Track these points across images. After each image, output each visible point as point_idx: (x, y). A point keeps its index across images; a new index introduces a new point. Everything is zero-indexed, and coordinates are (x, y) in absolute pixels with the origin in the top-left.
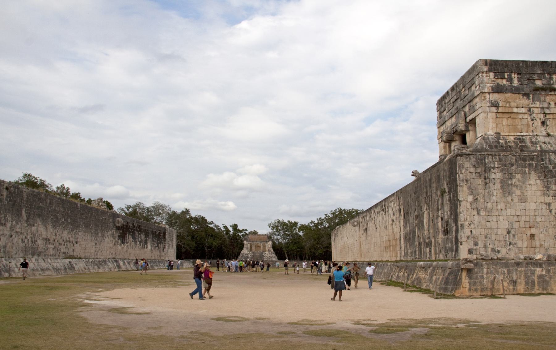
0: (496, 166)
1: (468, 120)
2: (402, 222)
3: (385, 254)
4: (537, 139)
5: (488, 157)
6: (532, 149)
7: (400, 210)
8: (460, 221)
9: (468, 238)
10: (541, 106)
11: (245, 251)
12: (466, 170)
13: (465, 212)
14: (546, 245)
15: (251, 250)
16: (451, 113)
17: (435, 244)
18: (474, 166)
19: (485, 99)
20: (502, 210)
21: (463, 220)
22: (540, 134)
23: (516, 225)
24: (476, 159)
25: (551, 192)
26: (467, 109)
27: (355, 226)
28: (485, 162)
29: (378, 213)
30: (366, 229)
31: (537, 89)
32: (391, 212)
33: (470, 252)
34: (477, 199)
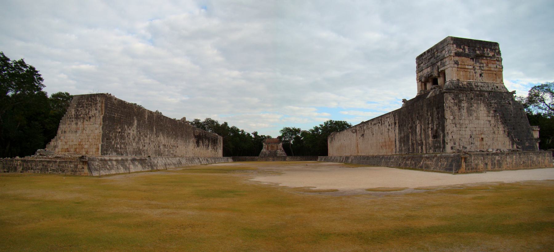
1: (440, 70)
2: (397, 131)
3: (381, 151)
6: (476, 89)
7: (395, 123)
9: (451, 140)
11: (264, 150)
13: (449, 126)
14: (489, 144)
15: (268, 149)
17: (426, 145)
18: (453, 99)
23: (474, 133)
25: (491, 115)
26: (439, 64)
27: (354, 133)
29: (374, 124)
30: (363, 135)
32: (387, 124)
33: (452, 148)
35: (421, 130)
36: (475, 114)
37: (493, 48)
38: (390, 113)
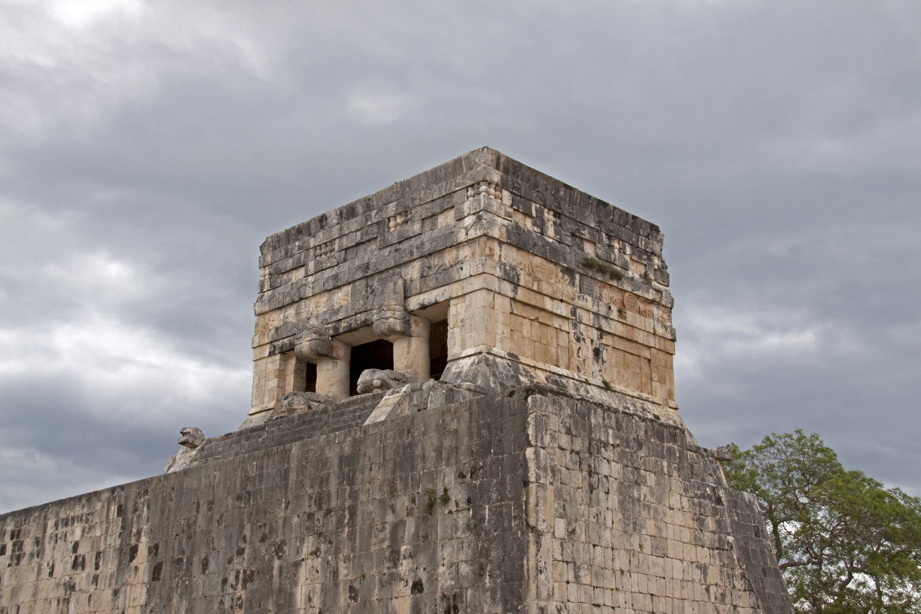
0: (611, 442)
1: (414, 303)
4: (588, 393)
5: (595, 412)
8: (538, 596)
10: (595, 309)
12: (553, 438)
16: (336, 277)
18: (569, 431)
19: (491, 256)
20: (622, 572)
21: (544, 594)
22: (591, 381)
24: (572, 409)
26: (413, 271)
28: (590, 424)
31: (588, 264)
32: (59, 556)
34: (574, 531)
35: (329, 591)
36: (650, 527)
37: (642, 245)
38: (91, 497)
